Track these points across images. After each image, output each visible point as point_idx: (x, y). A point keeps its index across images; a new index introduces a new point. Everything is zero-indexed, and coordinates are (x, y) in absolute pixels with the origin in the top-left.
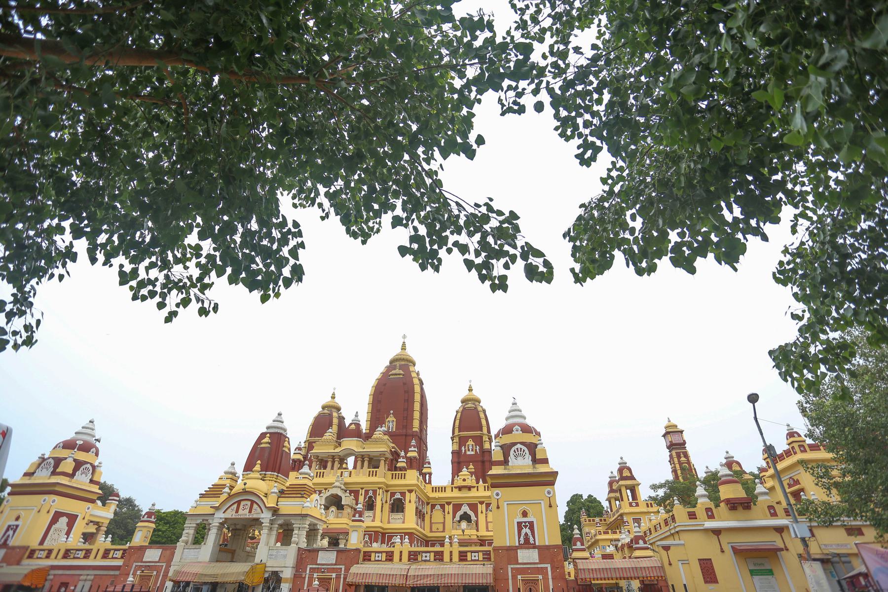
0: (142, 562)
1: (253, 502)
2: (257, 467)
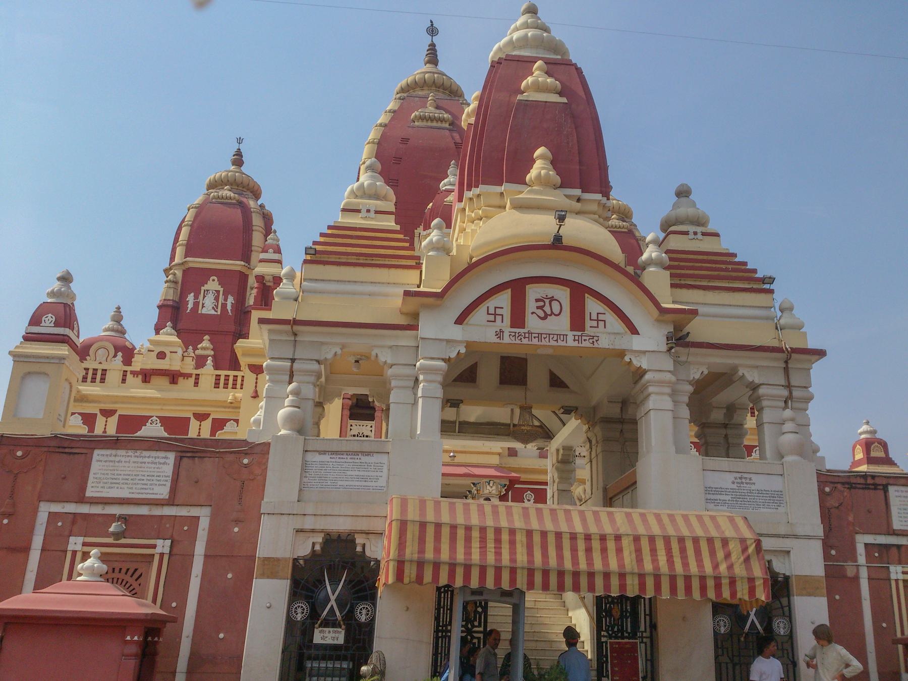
0: (81, 499)
1: (579, 292)
2: (539, 168)
